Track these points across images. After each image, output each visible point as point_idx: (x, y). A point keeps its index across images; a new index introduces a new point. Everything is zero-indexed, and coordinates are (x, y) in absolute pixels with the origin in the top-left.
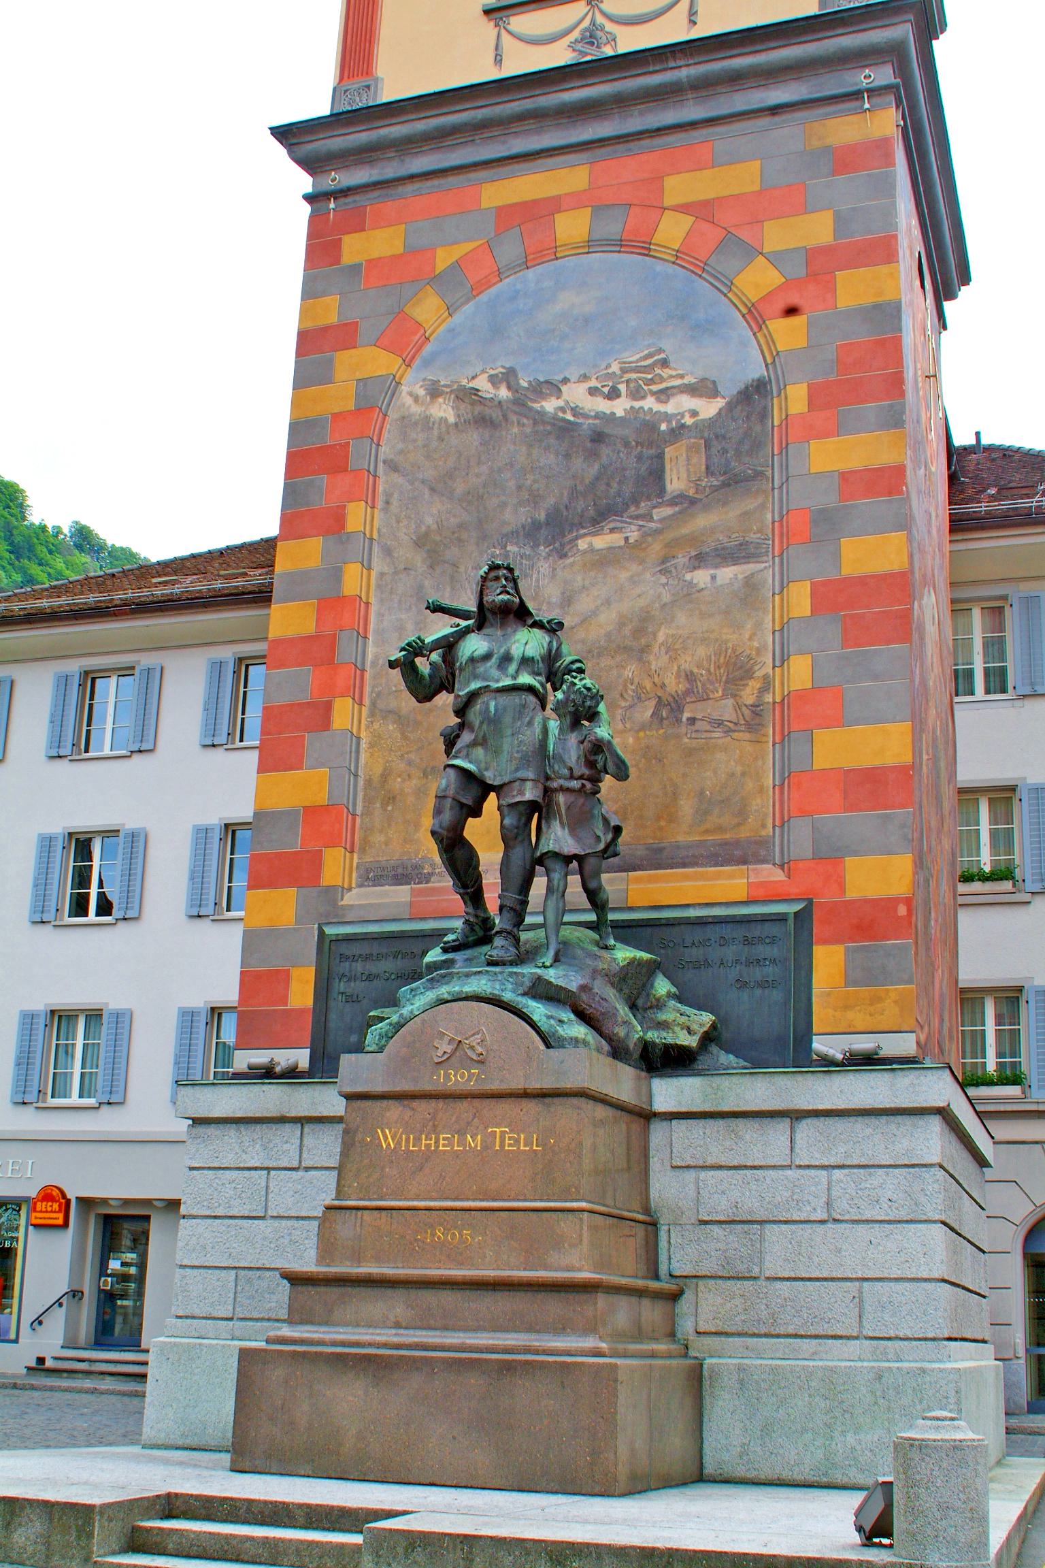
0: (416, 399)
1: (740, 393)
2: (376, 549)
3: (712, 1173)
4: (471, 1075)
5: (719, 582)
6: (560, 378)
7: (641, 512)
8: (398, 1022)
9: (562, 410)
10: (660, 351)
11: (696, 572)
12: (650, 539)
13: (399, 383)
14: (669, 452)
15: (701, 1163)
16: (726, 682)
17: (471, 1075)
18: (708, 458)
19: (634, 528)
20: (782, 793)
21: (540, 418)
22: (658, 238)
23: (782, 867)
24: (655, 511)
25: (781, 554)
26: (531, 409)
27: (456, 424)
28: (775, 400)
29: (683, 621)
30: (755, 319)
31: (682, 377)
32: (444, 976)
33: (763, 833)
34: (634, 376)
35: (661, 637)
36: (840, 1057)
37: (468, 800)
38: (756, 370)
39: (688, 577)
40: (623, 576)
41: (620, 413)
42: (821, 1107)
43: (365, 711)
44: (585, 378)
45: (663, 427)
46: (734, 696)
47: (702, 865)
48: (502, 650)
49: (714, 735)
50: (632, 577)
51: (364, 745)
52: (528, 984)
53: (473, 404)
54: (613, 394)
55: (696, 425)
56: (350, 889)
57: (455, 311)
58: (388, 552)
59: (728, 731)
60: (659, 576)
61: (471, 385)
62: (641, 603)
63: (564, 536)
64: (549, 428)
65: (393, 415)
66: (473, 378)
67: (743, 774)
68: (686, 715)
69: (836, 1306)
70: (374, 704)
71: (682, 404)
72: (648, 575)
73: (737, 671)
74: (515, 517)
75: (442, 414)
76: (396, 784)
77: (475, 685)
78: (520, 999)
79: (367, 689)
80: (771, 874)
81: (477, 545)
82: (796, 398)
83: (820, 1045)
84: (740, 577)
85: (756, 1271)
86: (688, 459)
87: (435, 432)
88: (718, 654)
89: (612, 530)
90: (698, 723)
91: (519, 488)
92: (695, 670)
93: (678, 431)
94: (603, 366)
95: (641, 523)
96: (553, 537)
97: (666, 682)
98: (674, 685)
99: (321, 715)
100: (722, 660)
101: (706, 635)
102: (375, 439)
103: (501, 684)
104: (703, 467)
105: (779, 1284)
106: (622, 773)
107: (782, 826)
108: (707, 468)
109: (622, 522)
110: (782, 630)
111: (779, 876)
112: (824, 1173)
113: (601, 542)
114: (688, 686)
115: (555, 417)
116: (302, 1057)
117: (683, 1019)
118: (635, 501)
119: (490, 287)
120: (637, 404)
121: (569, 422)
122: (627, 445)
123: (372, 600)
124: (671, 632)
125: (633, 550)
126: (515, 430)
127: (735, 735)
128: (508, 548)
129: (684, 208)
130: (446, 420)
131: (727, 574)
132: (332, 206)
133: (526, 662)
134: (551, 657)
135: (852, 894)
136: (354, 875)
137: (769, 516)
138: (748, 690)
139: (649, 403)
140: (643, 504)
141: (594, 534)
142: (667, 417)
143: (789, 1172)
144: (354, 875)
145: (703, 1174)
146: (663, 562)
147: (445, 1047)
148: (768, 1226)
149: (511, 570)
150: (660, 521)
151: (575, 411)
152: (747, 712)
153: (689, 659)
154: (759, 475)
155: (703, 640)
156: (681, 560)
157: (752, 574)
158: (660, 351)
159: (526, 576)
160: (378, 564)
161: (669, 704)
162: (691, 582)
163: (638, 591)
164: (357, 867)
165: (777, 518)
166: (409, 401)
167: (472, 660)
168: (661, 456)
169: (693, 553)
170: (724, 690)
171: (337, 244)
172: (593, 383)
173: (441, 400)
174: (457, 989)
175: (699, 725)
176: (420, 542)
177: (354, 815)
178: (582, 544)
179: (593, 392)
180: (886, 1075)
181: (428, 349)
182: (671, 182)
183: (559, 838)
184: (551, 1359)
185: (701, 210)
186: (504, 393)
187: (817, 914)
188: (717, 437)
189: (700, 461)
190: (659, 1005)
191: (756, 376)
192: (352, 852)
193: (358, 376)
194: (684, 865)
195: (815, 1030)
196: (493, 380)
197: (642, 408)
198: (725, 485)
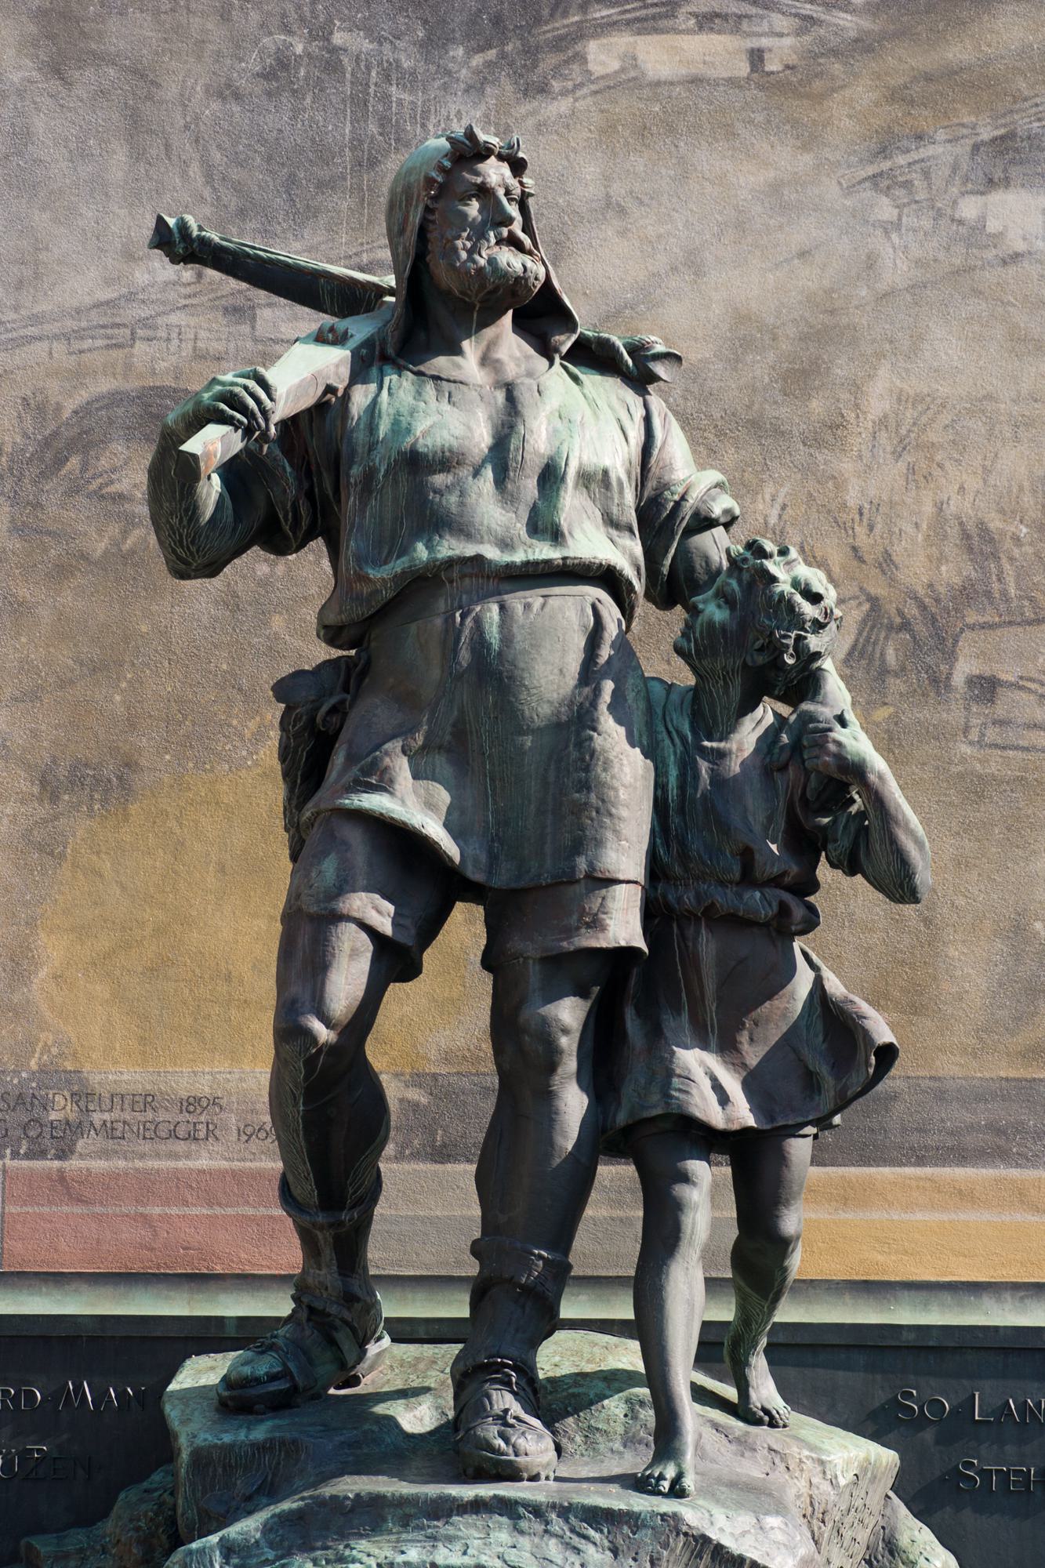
11: (997, 197)
12: (837, 68)
19: (780, 22)
35: (877, 402)
40: (748, 179)
50: (775, 188)
60: (867, 194)
62: (809, 278)
63: (538, 21)
68: (964, 668)
72: (830, 190)
77: (450, 547)
92: (995, 524)
96: (497, 21)
97: (898, 550)
98: (925, 568)
103: (519, 557)
114: (969, 570)
124: (914, 385)
128: (338, 38)
146: (883, 152)
153: (973, 483)
161: (905, 626)
169: (986, 134)
178: (603, 56)
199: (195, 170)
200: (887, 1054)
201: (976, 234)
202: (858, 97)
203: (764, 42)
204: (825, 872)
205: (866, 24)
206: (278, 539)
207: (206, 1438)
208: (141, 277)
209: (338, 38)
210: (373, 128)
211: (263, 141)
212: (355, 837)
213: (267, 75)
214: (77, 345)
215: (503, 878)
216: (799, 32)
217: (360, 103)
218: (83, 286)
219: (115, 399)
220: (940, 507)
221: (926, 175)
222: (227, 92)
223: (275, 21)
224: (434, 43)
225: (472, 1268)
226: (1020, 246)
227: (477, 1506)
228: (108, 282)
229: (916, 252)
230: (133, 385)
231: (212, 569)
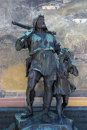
11: (76, 19)
12: (63, 9)
19: (58, 5)
29: (73, 32)
35: (67, 36)
39: (74, 20)
40: (56, 18)
48: (45, 40)
49: (82, 63)
50: (58, 18)
62: (61, 26)
68: (75, 57)
72: (63, 19)
81: (12, 3)
88: (83, 42)
89: (52, 5)
90: (78, 59)
95: (60, 4)
96: (35, 4)
100: (84, 43)
101: (79, 36)
109: (55, 3)
113: (49, 8)
114: (75, 49)
125: (59, 11)
128: (22, 6)
141: (47, 5)
146: (66, 16)
149: (44, 17)
150: (66, 4)
155: (78, 38)
156: (71, 15)
159: (28, 15)
162: (74, 22)
163: (60, 23)
170: (84, 51)
178: (44, 8)
199: (11, 17)
202: (65, 11)
203: (57, 6)
205: (65, 5)
206: (24, 47)
207: (21, 121)
209: (22, 6)
210: (25, 13)
211: (16, 14)
212: (34, 71)
213: (16, 9)
214: (2, 31)
215: (46, 75)
216: (59, 6)
217: (24, 11)
220: (72, 44)
221: (70, 17)
222: (13, 10)
223: (17, 5)
224: (30, 6)
226: (78, 23)
228: (4, 26)
229: (69, 24)
230: (6, 34)
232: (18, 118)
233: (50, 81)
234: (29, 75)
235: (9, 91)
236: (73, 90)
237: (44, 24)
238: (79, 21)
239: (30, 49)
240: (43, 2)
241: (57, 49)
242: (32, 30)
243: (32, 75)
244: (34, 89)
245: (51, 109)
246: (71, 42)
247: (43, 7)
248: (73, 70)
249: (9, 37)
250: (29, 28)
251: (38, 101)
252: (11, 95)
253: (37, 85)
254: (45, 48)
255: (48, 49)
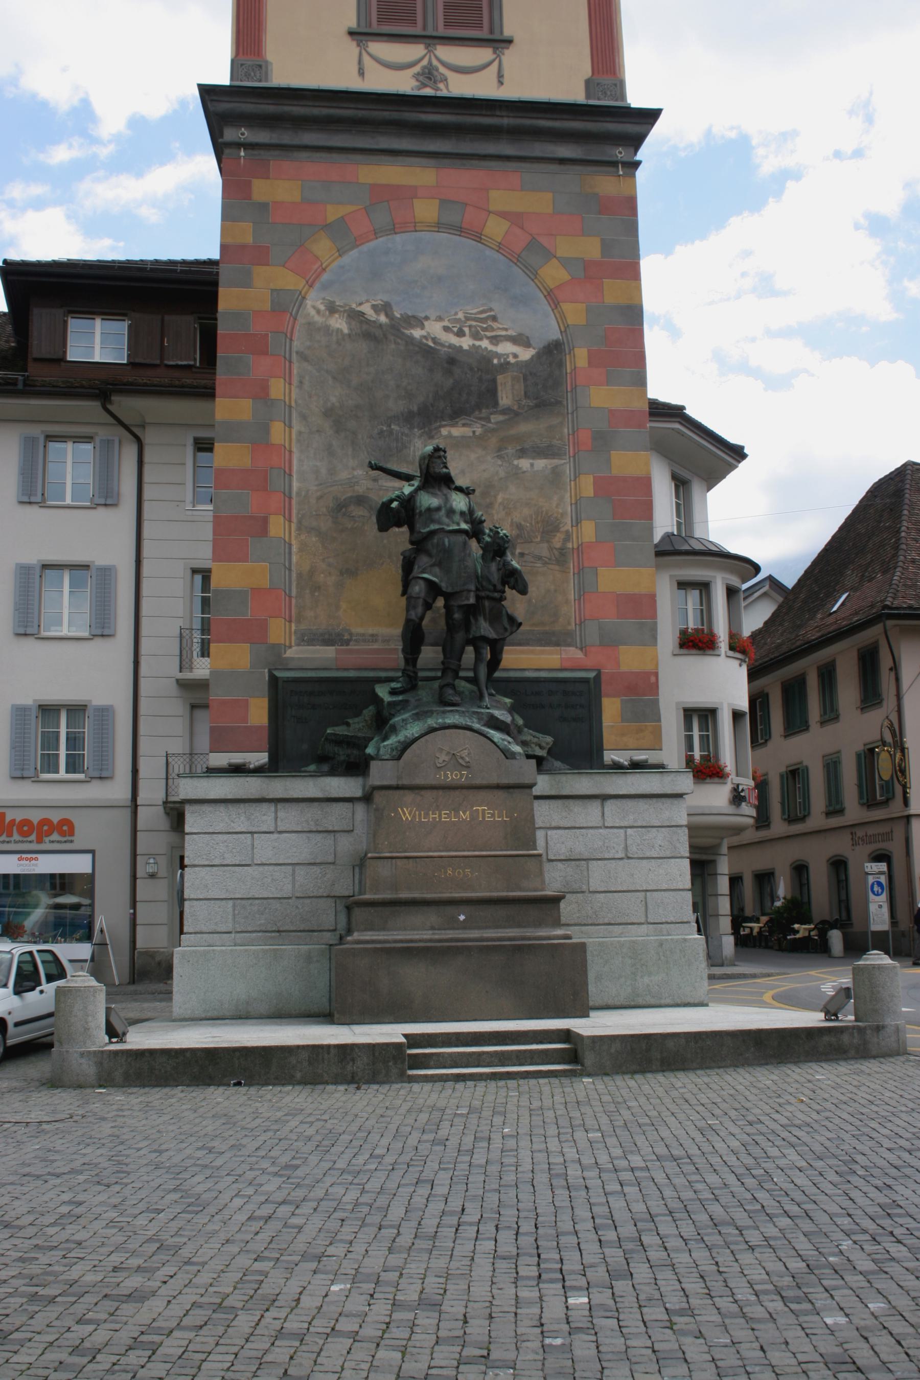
0: (318, 312)
1: (544, 347)
2: (294, 414)
3: (555, 831)
4: (462, 775)
5: (536, 468)
6: (423, 315)
7: (483, 415)
8: (404, 741)
9: (425, 337)
10: (491, 310)
13: (304, 298)
14: (500, 379)
15: (548, 825)
16: (543, 532)
17: (462, 775)
18: (526, 387)
19: (478, 425)
20: (580, 604)
21: (410, 340)
22: (487, 231)
23: (581, 649)
24: (492, 416)
25: (574, 457)
26: (403, 334)
27: (349, 335)
28: (568, 356)
30: (552, 299)
31: (506, 330)
32: (426, 712)
33: (569, 628)
34: (474, 323)
36: (626, 763)
37: (430, 601)
38: (554, 333)
40: (473, 456)
41: (466, 347)
42: (621, 793)
43: (294, 526)
44: (440, 319)
45: (495, 361)
46: (548, 542)
47: (532, 645)
51: (295, 549)
52: (485, 718)
53: (361, 322)
54: (460, 334)
55: (517, 363)
56: (290, 647)
57: (344, 253)
58: (304, 417)
59: (545, 563)
61: (359, 309)
64: (417, 349)
65: (301, 320)
66: (361, 304)
67: (555, 591)
68: (518, 551)
69: (632, 907)
70: (300, 522)
71: (506, 348)
72: (489, 458)
73: (549, 526)
74: (396, 406)
75: (338, 326)
76: (321, 578)
78: (483, 728)
79: (294, 512)
80: (573, 653)
82: (580, 357)
83: (610, 756)
84: (549, 467)
85: (584, 888)
86: (513, 386)
87: (334, 338)
89: (464, 425)
91: (398, 386)
92: (523, 523)
93: (505, 366)
94: (453, 313)
99: (261, 527)
102: (289, 335)
104: (523, 393)
105: (598, 895)
106: (523, 591)
107: (580, 625)
108: (525, 393)
110: (576, 503)
111: (579, 655)
112: (622, 831)
113: (457, 432)
115: (421, 342)
116: (261, 758)
117: (535, 740)
118: (478, 407)
119: (368, 241)
120: (477, 343)
121: (430, 347)
122: (471, 369)
123: (294, 449)
125: (480, 440)
126: (393, 346)
127: (550, 566)
128: (393, 427)
129: (503, 215)
130: (342, 331)
131: (541, 464)
132: (242, 154)
133: (462, 514)
134: (471, 511)
135: (624, 668)
136: (293, 638)
137: (566, 430)
138: (557, 539)
139: (485, 344)
140: (484, 411)
141: (452, 426)
142: (498, 355)
143: (601, 831)
144: (293, 638)
145: (549, 832)
147: (443, 757)
148: (590, 862)
149: (445, 452)
150: (497, 423)
151: (434, 340)
152: (556, 553)
154: (558, 403)
157: (556, 466)
158: (491, 310)
160: (297, 426)
164: (295, 632)
165: (571, 432)
166: (313, 312)
167: (429, 510)
168: (494, 381)
169: (519, 448)
171: (249, 184)
172: (446, 323)
173: (337, 316)
174: (440, 721)
175: (527, 558)
176: (328, 413)
177: (290, 597)
178: (444, 431)
179: (446, 329)
180: (658, 776)
181: (325, 277)
182: (493, 194)
183: (484, 628)
184: (545, 942)
185: (515, 219)
186: (383, 319)
187: (603, 678)
188: (531, 374)
189: (520, 387)
190: (520, 731)
191: (555, 338)
192: (290, 621)
193: (272, 286)
194: (520, 644)
195: (605, 747)
196: (374, 307)
197: (480, 346)
198: (537, 406)
200: (520, 624)
201: (517, 467)
202: (493, 441)
204: (507, 588)
208: (355, 473)
209: (393, 427)
212: (422, 582)
213: (379, 434)
215: (449, 590)
218: (344, 475)
219: (351, 497)
224: (411, 428)
225: (442, 667)
227: (452, 711)
231: (387, 530)
232: (382, 692)
233: (460, 607)
234: (409, 591)
235: (360, 630)
236: (515, 628)
237: (446, 468)
238: (529, 466)
239: (412, 529)
240: (442, 419)
241: (476, 531)
242: (416, 483)
243: (418, 588)
244: (420, 625)
245: (462, 674)
246: (508, 514)
247: (442, 430)
248: (514, 580)
249: (360, 500)
250: (408, 478)
251: (430, 655)
252: (364, 641)
253: (429, 615)
254: (448, 525)
255: (456, 527)
